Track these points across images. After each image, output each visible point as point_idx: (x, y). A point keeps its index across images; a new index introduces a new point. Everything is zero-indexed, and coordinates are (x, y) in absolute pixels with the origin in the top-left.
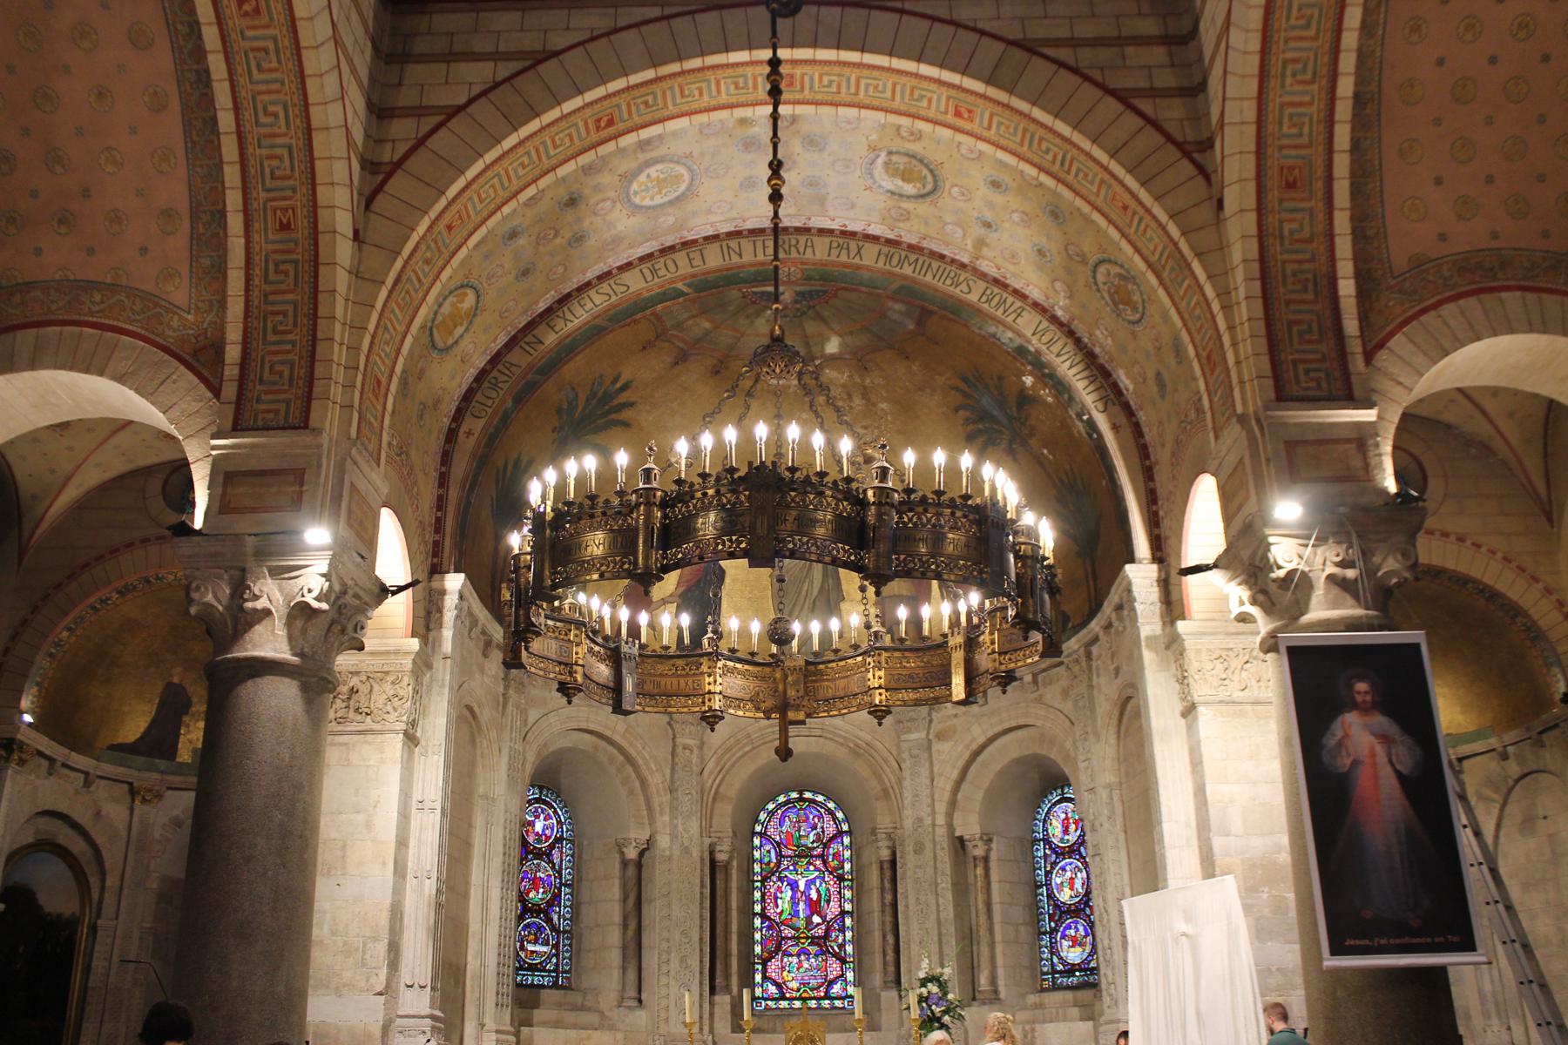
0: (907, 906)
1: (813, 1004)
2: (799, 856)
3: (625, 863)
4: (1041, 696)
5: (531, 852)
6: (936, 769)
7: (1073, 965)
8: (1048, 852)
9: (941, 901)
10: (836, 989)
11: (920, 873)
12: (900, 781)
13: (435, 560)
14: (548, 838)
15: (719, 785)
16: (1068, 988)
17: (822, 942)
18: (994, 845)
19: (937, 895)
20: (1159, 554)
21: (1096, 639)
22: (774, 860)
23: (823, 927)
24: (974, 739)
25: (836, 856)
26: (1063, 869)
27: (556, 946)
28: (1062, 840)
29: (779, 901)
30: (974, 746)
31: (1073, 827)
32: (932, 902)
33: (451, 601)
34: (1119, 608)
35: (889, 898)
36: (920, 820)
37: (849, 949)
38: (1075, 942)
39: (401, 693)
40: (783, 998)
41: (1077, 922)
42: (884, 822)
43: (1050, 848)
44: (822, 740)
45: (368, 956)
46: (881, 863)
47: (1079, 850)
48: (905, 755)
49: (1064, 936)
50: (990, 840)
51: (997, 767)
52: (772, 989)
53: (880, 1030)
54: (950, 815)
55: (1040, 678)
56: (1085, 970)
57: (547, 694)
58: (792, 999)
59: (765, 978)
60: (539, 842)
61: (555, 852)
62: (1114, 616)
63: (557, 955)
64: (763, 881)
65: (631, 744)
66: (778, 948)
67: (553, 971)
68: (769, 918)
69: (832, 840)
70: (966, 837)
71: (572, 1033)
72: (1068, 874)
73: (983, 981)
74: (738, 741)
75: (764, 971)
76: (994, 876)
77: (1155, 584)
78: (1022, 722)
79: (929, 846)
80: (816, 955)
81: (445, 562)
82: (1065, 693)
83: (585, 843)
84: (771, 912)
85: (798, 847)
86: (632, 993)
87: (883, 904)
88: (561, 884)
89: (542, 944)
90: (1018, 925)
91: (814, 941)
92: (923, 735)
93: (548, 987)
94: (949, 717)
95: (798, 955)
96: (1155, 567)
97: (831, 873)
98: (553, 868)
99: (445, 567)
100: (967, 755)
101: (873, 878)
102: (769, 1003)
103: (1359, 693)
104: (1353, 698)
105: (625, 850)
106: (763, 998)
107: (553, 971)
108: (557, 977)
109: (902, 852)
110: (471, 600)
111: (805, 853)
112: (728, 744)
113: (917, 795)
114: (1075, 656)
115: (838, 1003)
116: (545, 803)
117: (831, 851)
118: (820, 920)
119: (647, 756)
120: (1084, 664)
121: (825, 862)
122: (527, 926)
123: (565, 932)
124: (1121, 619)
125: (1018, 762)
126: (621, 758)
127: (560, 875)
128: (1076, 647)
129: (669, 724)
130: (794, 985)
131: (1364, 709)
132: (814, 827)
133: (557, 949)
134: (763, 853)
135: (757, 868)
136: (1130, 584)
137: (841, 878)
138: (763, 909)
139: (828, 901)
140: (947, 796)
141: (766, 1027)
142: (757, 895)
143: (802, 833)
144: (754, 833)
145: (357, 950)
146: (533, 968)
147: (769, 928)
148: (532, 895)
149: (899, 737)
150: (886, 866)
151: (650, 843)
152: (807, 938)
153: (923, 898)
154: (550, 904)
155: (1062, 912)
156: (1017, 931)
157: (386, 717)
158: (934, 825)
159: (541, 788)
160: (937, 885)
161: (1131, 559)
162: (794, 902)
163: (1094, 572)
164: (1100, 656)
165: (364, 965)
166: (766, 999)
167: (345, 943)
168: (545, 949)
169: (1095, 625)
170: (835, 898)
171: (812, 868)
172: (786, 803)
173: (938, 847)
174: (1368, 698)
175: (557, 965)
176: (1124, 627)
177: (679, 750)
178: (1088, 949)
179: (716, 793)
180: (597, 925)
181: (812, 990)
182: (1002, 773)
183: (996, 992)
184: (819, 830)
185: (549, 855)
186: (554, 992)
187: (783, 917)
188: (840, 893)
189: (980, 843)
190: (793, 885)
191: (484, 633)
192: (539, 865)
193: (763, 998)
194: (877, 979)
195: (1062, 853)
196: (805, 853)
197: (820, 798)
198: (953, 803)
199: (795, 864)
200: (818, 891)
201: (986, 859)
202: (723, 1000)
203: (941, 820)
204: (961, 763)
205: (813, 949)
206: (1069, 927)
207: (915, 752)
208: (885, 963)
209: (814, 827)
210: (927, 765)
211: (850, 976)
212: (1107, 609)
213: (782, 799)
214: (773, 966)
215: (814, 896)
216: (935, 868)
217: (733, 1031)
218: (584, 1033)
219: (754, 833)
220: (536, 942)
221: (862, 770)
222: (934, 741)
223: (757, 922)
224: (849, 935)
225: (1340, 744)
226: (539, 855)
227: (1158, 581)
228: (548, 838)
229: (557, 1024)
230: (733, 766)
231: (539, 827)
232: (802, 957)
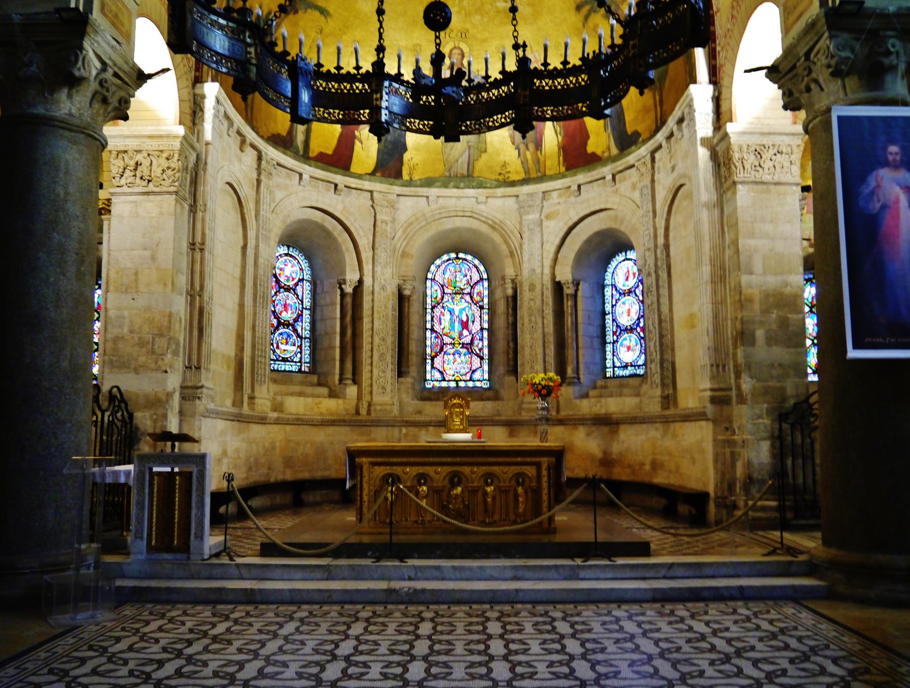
0: (523, 324)
1: (462, 384)
2: (456, 294)
3: (343, 295)
4: (617, 190)
5: (283, 287)
6: (544, 239)
7: (627, 363)
8: (614, 292)
9: (545, 321)
10: (477, 376)
11: (532, 304)
12: (521, 245)
13: (197, 74)
14: (293, 279)
15: (406, 246)
16: (623, 377)
17: (469, 347)
18: (580, 287)
19: (543, 318)
20: (714, 79)
21: (660, 147)
22: (439, 296)
23: (470, 337)
24: (570, 218)
25: (479, 294)
26: (624, 303)
27: (300, 347)
28: (624, 285)
29: (443, 321)
30: (570, 223)
31: (631, 277)
32: (540, 321)
33: (209, 105)
34: (681, 121)
35: (511, 319)
36: (534, 270)
37: (486, 351)
38: (629, 348)
39: (173, 165)
40: (444, 380)
41: (630, 336)
42: (510, 272)
43: (616, 290)
44: (471, 219)
45: (156, 347)
46: (507, 298)
47: (635, 291)
48: (525, 229)
49: (622, 345)
50: (578, 284)
51: (585, 237)
52: (438, 376)
53: (503, 400)
54: (553, 267)
55: (617, 177)
56: (635, 366)
57: (288, 182)
58: (449, 381)
59: (433, 367)
60: (288, 280)
61: (299, 288)
62: (675, 128)
63: (301, 353)
64: (432, 309)
65: (347, 218)
66: (442, 349)
67: (298, 362)
68: (436, 332)
69: (476, 284)
70: (562, 282)
71: (310, 400)
72: (626, 307)
73: (570, 371)
74: (417, 219)
76: (580, 307)
77: (710, 100)
78: (603, 207)
79: (538, 287)
80: (465, 355)
81: (204, 75)
82: (634, 187)
83: (318, 282)
84: (437, 328)
85: (455, 288)
86: (349, 375)
87: (508, 323)
88: (303, 308)
90: (593, 337)
91: (464, 346)
92: (537, 216)
93: (295, 372)
94: (554, 205)
95: (454, 354)
96: (711, 87)
97: (475, 304)
98: (298, 297)
99: (204, 78)
100: (565, 229)
101: (501, 307)
102: (435, 383)
103: (891, 154)
104: (886, 159)
105: (343, 286)
107: (298, 362)
108: (301, 366)
109: (521, 290)
110: (226, 105)
111: (460, 292)
112: (410, 220)
113: (532, 254)
114: (643, 160)
115: (478, 384)
116: (291, 256)
117: (476, 291)
118: (468, 334)
119: (358, 226)
120: (649, 166)
121: (471, 298)
122: (281, 334)
123: (305, 338)
124: (680, 129)
125: (598, 234)
126: (340, 227)
127: (302, 301)
128: (644, 154)
129: (372, 206)
130: (451, 372)
131: (896, 166)
132: (466, 276)
133: (301, 349)
134: (432, 291)
135: (429, 300)
136: (692, 100)
137: (482, 308)
138: (432, 326)
139: (473, 322)
140: (551, 255)
141: (433, 397)
142: (429, 318)
143: (457, 279)
144: (427, 279)
145: (148, 342)
146: (285, 360)
148: (284, 314)
149: (521, 217)
150: (510, 300)
151: (361, 282)
152: (460, 344)
153: (533, 319)
154: (296, 320)
155: (621, 330)
156: (592, 342)
157: (163, 182)
158: (542, 273)
159: (289, 247)
160: (543, 311)
161: (695, 82)
162: (452, 322)
163: (661, 101)
164: (661, 159)
165: (153, 352)
167: (140, 339)
168: (294, 348)
169: (660, 137)
170: (478, 319)
171: (463, 300)
172: (448, 260)
173: (545, 287)
174: (898, 158)
175: (301, 358)
176: (682, 136)
177: (378, 223)
178: (637, 353)
179: (404, 252)
180: (326, 334)
181: (462, 375)
182: (589, 241)
183: (578, 379)
184: (468, 277)
185: (294, 290)
186: (299, 374)
187: (445, 331)
188: (480, 317)
189: (571, 286)
190: (451, 312)
191: (239, 133)
192: (288, 296)
194: (501, 370)
195: (623, 294)
196: (460, 292)
197: (469, 257)
198: (555, 260)
199: (452, 298)
200: (467, 315)
201: (575, 296)
202: (408, 380)
203: (547, 271)
204: (561, 234)
205: (464, 351)
206: (625, 339)
207: (531, 226)
208: (508, 359)
209: (466, 276)
210: (539, 235)
211: (486, 367)
212: (671, 122)
213: (445, 257)
214: (438, 361)
215: (465, 319)
216: (543, 301)
217: (413, 399)
218: (317, 400)
219: (427, 279)
220: (287, 343)
221: (497, 238)
222: (544, 220)
223: (428, 333)
224: (486, 343)
225: (872, 193)
226: (288, 289)
227: (712, 98)
229: (301, 394)
230: (414, 235)
231: (288, 271)
232: (457, 356)
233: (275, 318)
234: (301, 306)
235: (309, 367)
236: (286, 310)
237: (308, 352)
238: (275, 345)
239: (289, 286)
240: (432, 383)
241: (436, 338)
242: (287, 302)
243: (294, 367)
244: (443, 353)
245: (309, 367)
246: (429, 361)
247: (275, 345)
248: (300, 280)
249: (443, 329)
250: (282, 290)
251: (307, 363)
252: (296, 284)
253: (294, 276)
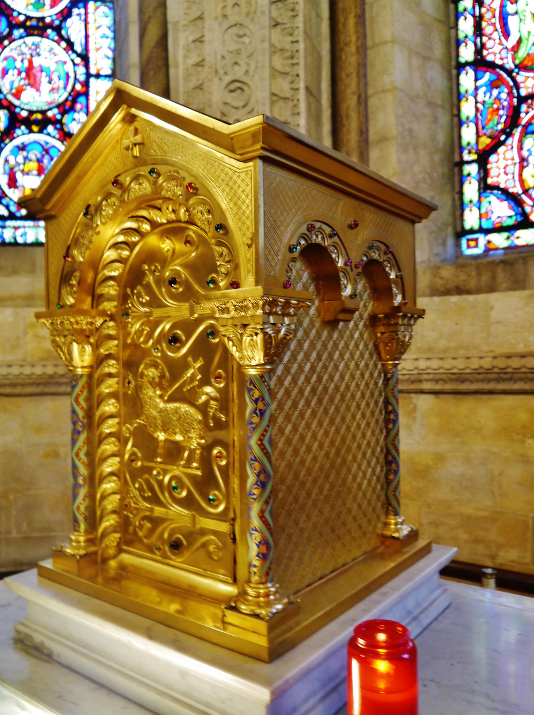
68: (492, 66)
75: (484, 173)
88: (88, 75)
106: (482, 231)
122: (22, 148)
127: (85, 58)
138: (478, 51)
141: (473, 283)
147: (493, 85)
166: (487, 232)
185: (58, 29)
187: (522, 54)
193: (482, 231)
234: (81, 70)
236: (34, 84)
239: (42, 19)
240: (482, 239)
241: (493, 85)
242: (36, 62)
244: (517, 132)
246: (472, 169)
249: (516, 49)
250: (17, 33)
252: (66, 14)
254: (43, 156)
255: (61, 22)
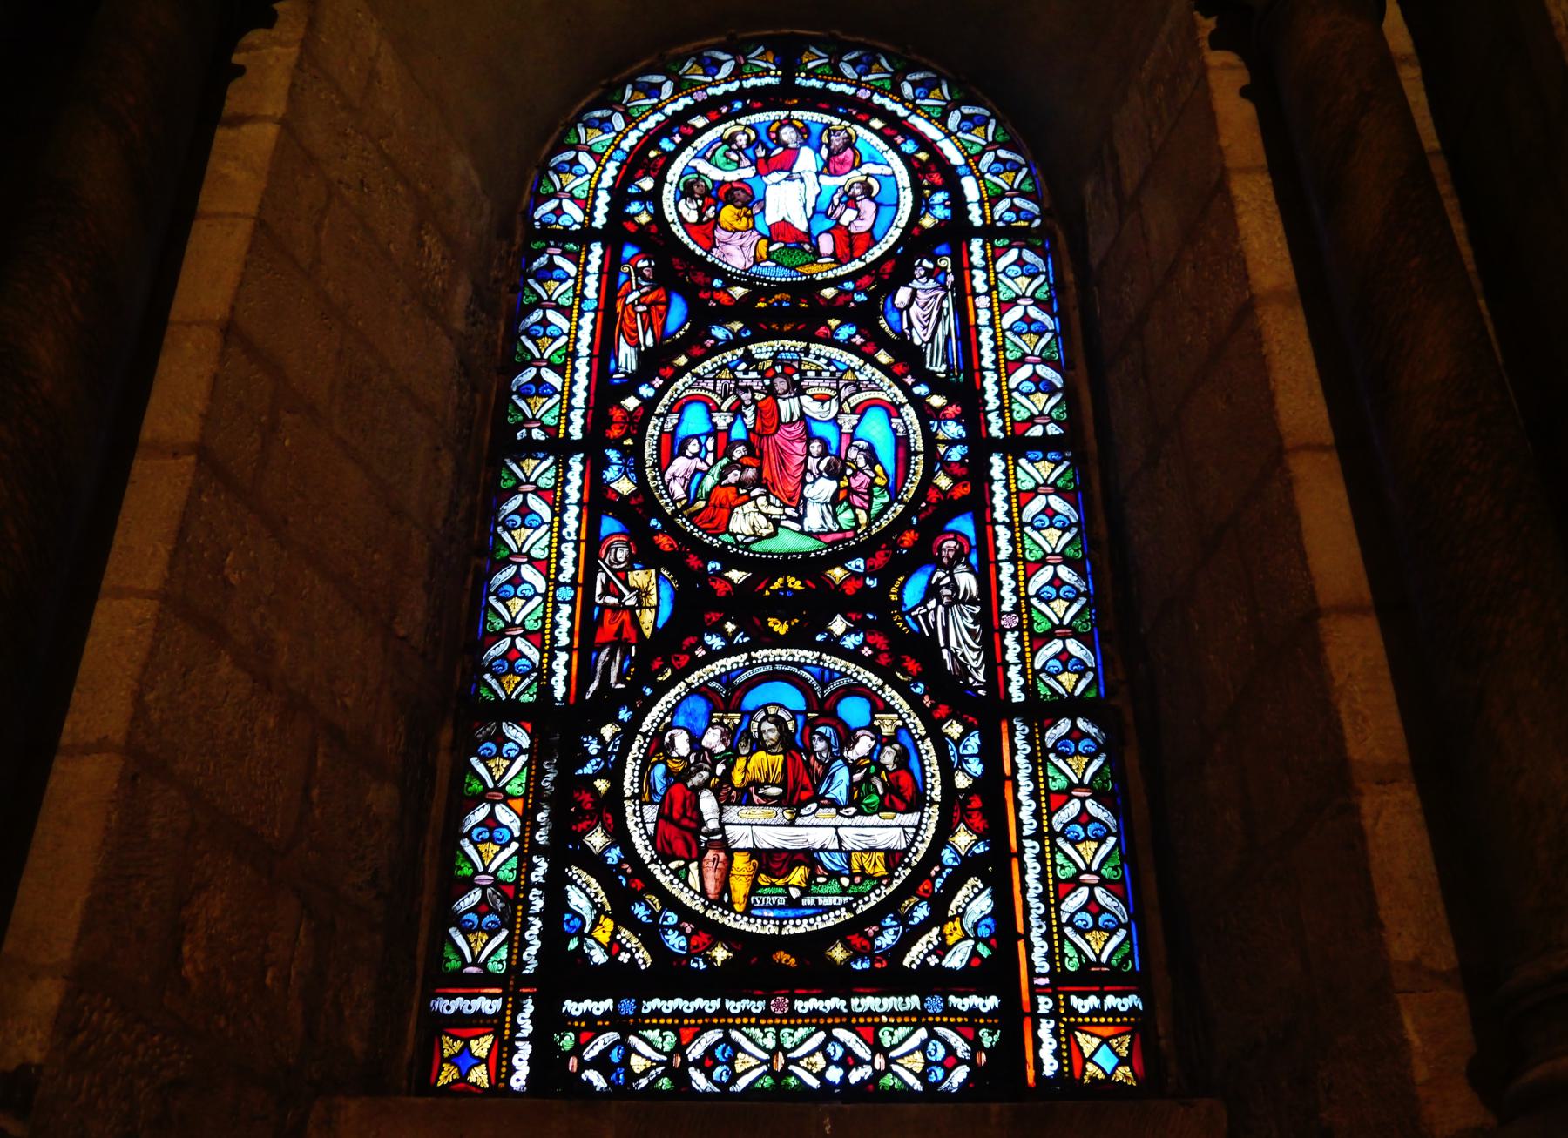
67: (971, 979)
88: (980, 445)
89: (856, 802)
107: (971, 979)
116: (814, 100)
133: (994, 828)
148: (743, 522)
168: (887, 831)
185: (865, 318)
228: (849, 244)
233: (645, 556)
235: (1135, 1024)
237: (1092, 854)
238: (641, 823)
243: (907, 1043)
245: (1135, 1024)
247: (641, 823)
248: (916, 242)
251: (1092, 978)
253: (859, 219)
254: (811, 726)
255: (873, 297)
